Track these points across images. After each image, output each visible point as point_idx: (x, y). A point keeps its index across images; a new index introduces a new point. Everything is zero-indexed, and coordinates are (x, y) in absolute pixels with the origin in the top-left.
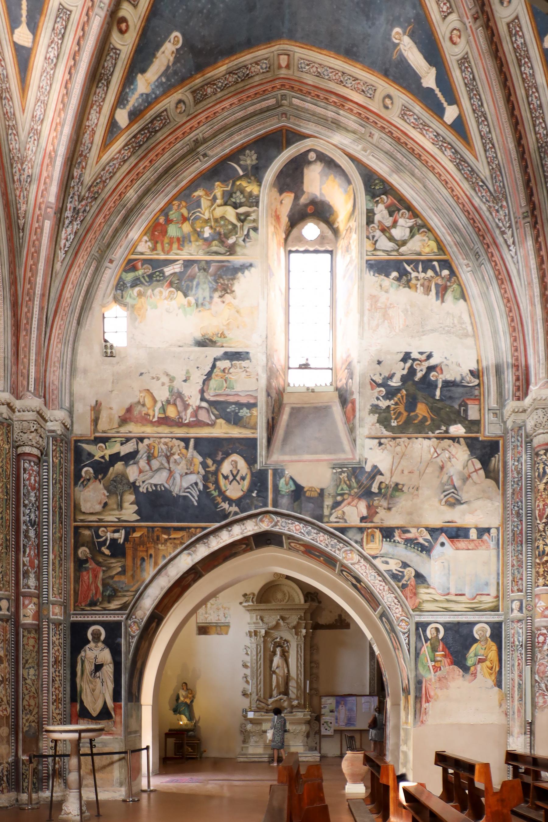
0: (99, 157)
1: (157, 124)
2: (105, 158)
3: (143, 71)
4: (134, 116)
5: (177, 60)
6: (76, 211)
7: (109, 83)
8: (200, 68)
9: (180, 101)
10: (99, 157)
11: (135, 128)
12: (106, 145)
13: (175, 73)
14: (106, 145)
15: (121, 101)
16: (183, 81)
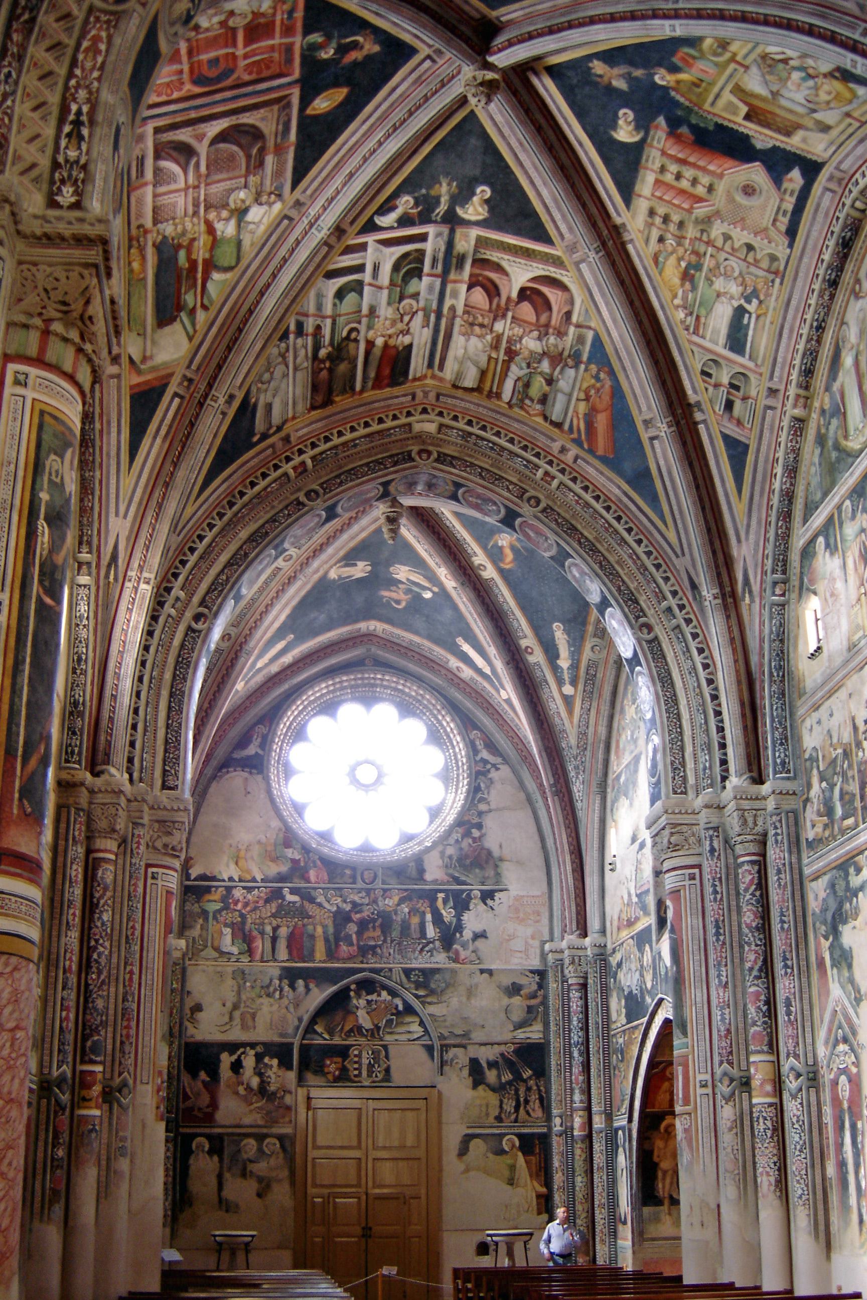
0: (572, 723)
1: (592, 672)
2: (576, 720)
3: (557, 657)
4: (574, 682)
5: (568, 634)
6: (576, 768)
7: (546, 681)
8: (584, 623)
9: (592, 648)
10: (572, 723)
11: (580, 687)
12: (570, 712)
13: (574, 639)
14: (570, 712)
15: (560, 682)
16: (582, 638)
